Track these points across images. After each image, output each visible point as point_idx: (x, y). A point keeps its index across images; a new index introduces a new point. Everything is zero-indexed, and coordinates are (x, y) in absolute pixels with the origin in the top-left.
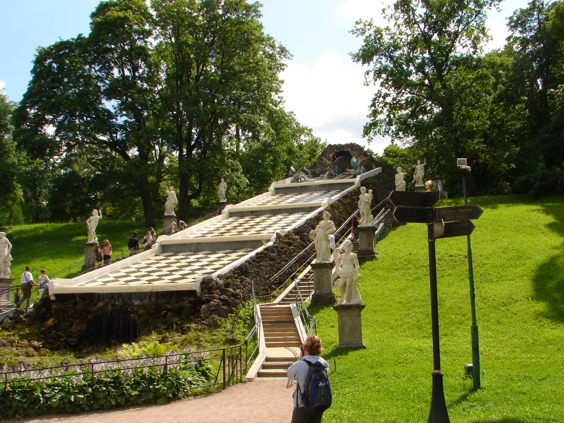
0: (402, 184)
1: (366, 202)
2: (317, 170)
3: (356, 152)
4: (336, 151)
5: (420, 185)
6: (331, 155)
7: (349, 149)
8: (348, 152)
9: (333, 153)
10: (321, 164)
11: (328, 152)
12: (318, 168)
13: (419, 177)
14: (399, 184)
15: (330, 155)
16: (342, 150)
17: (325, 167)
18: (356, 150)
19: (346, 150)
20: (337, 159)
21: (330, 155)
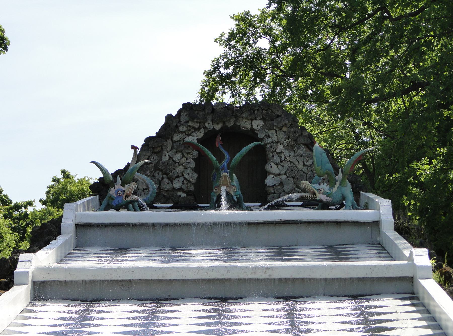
4: (209, 125)
7: (257, 124)
9: (201, 134)
10: (156, 168)
11: (181, 129)
16: (231, 124)
17: (171, 180)
19: (245, 124)
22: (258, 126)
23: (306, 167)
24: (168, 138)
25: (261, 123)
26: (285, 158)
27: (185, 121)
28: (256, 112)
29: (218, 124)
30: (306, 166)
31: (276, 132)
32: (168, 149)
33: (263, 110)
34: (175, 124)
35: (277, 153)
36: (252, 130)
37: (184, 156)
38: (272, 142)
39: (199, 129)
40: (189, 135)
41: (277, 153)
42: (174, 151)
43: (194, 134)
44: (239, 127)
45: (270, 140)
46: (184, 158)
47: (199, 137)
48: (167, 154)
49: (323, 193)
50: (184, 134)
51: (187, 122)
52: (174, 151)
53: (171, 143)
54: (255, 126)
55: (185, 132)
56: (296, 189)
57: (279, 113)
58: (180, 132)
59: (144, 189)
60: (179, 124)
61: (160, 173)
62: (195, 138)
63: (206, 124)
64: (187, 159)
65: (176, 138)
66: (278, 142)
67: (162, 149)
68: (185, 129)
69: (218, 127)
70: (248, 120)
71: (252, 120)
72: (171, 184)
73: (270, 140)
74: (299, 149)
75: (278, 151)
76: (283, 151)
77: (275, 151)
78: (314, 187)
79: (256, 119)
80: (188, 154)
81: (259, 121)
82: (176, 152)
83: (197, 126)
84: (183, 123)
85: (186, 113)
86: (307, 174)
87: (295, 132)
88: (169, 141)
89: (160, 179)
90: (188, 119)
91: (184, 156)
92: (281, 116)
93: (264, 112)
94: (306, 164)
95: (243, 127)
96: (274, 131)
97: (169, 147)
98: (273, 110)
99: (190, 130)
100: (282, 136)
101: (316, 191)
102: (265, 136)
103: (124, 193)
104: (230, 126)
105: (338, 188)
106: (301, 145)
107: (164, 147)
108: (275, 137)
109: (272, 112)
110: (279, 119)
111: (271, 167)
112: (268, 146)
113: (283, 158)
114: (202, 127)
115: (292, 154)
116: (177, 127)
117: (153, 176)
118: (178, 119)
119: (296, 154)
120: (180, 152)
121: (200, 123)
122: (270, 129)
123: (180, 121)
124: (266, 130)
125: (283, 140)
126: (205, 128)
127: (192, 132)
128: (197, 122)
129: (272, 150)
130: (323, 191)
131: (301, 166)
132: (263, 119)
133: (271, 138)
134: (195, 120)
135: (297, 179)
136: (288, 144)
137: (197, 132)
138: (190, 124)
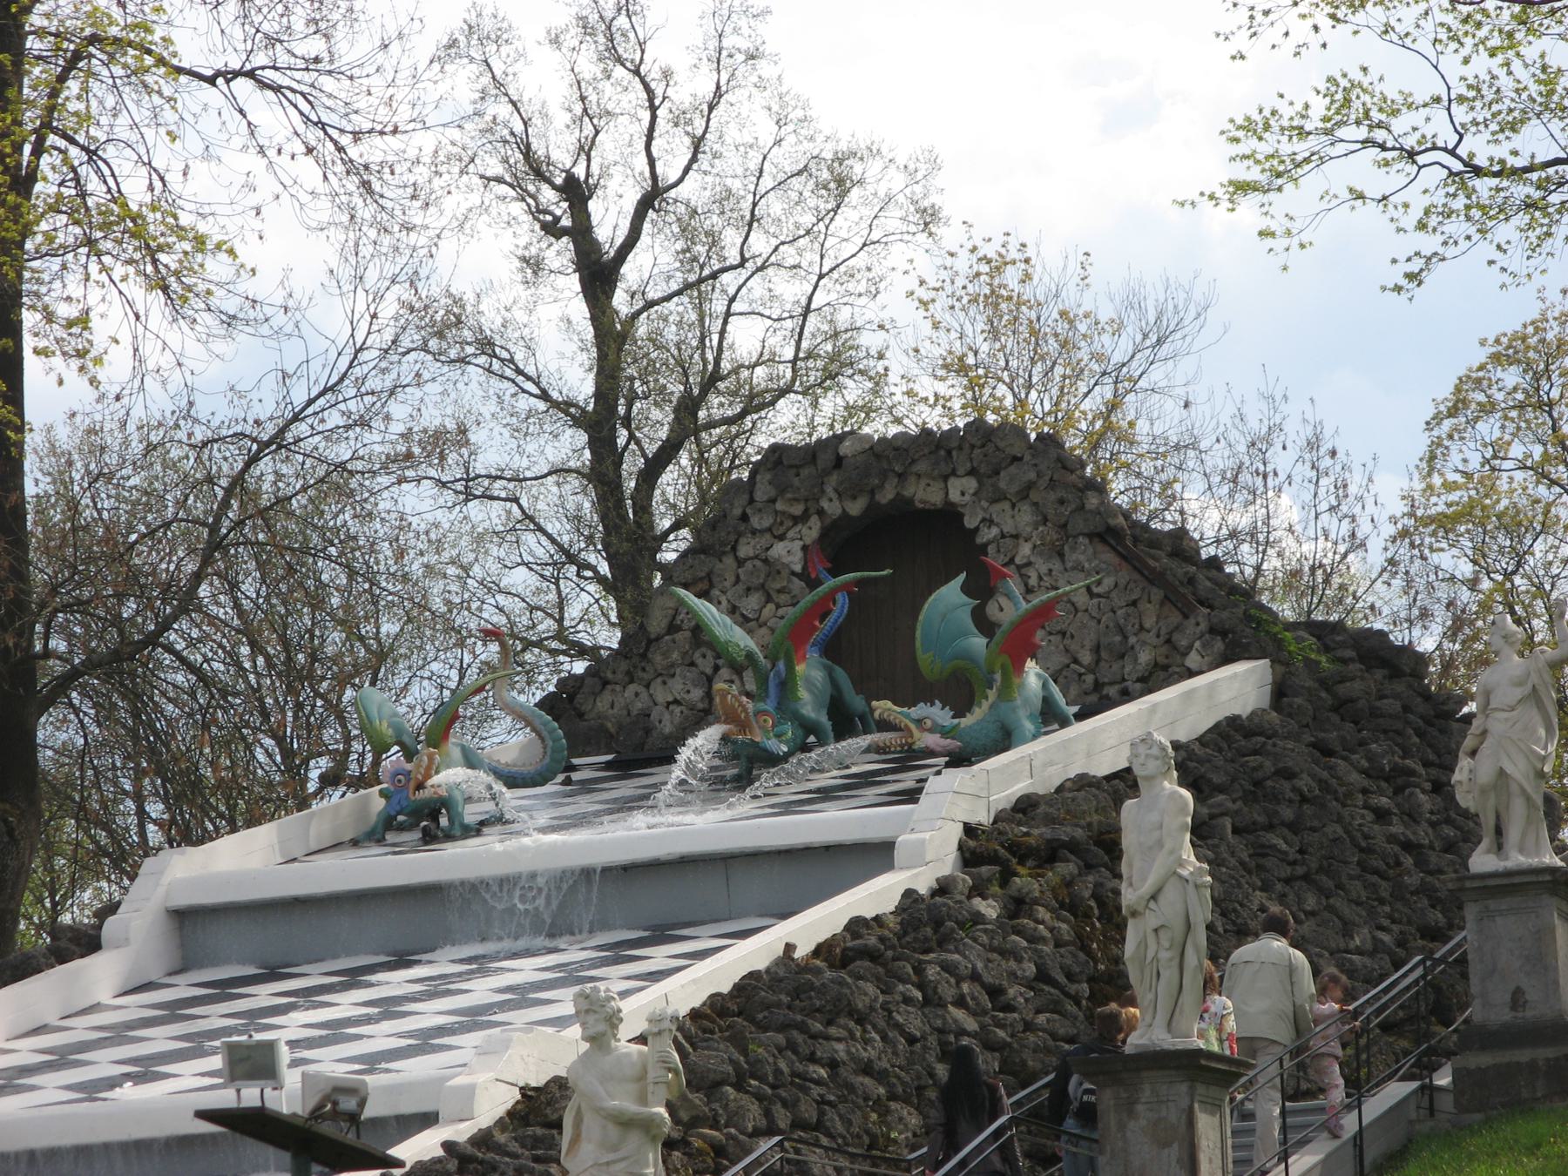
0: (1171, 895)
1: (627, 1123)
2: (661, 695)
3: (1025, 517)
4: (832, 507)
5: (1517, 859)
6: (789, 552)
7: (960, 489)
8: (949, 515)
9: (812, 530)
11: (755, 522)
12: (667, 674)
13: (1502, 773)
14: (1147, 888)
15: (779, 550)
16: (887, 495)
18: (1024, 493)
19: (926, 494)
20: (831, 583)
21: (779, 550)
22: (963, 494)
23: (1095, 601)
24: (724, 553)
25: (971, 484)
26: (1040, 578)
27: (765, 498)
28: (954, 453)
29: (854, 498)
30: (1099, 596)
31: (1013, 506)
32: (727, 584)
33: (973, 447)
34: (737, 512)
35: (1019, 568)
36: (949, 504)
37: (769, 599)
38: (1003, 536)
39: (803, 518)
40: (781, 538)
41: (1019, 568)
42: (741, 588)
43: (791, 534)
44: (910, 501)
45: (995, 531)
46: (771, 606)
47: (808, 541)
48: (723, 599)
49: (931, 731)
50: (768, 536)
51: (773, 501)
52: (741, 588)
53: (735, 565)
54: (954, 496)
55: (769, 530)
56: (1073, 666)
57: (1017, 452)
58: (754, 532)
59: (669, 704)
60: (749, 511)
61: (710, 654)
62: (798, 544)
63: (825, 504)
64: (778, 606)
65: (744, 551)
66: (1016, 537)
67: (712, 585)
68: (767, 522)
69: (855, 508)
70: (934, 479)
71: (945, 478)
72: (737, 681)
73: (995, 531)
74: (1073, 549)
75: (1018, 560)
76: (1032, 559)
77: (1012, 561)
78: (907, 716)
79: (954, 473)
80: (779, 591)
81: (964, 480)
82: (749, 589)
83: (797, 510)
84: (759, 505)
85: (768, 476)
86: (1099, 622)
87: (1062, 502)
88: (729, 561)
89: (709, 671)
90: (773, 493)
91: (769, 599)
92: (1020, 459)
93: (977, 451)
94: (1095, 590)
95: (922, 502)
96: (1006, 505)
97: (731, 579)
98: (1001, 444)
99: (782, 523)
100: (1025, 517)
101: (912, 726)
102: (984, 520)
103: (409, 780)
104: (884, 501)
105: (991, 707)
106: (1081, 539)
107: (715, 580)
108: (1010, 521)
109: (998, 449)
110: (1013, 469)
111: (1001, 610)
112: (991, 549)
113: (1033, 581)
114: (812, 510)
115: (1056, 565)
116: (744, 518)
117: (692, 664)
118: (746, 497)
119: (1069, 565)
120: (757, 589)
121: (806, 500)
122: (994, 501)
123: (752, 501)
124: (985, 504)
125: (1029, 529)
126: (821, 513)
127: (789, 529)
128: (796, 500)
129: (1002, 559)
130: (929, 723)
131: (1081, 599)
132: (972, 472)
133: (997, 525)
134: (789, 495)
135: (1072, 637)
136: (1042, 538)
137: (799, 526)
138: (779, 506)
